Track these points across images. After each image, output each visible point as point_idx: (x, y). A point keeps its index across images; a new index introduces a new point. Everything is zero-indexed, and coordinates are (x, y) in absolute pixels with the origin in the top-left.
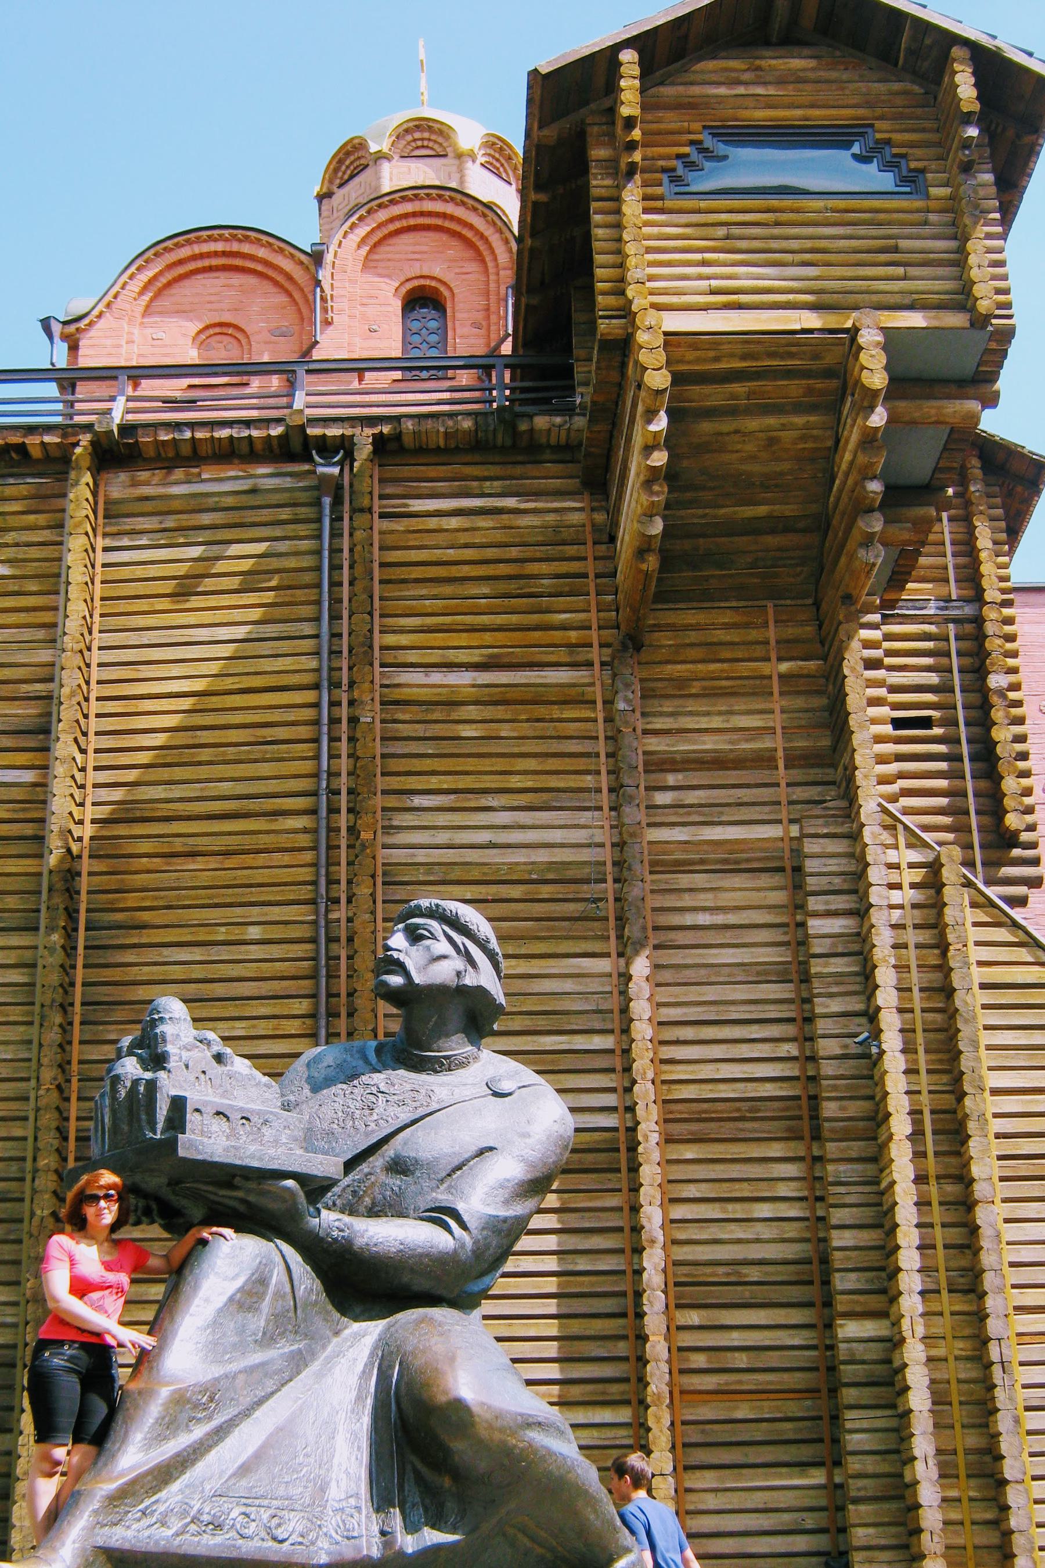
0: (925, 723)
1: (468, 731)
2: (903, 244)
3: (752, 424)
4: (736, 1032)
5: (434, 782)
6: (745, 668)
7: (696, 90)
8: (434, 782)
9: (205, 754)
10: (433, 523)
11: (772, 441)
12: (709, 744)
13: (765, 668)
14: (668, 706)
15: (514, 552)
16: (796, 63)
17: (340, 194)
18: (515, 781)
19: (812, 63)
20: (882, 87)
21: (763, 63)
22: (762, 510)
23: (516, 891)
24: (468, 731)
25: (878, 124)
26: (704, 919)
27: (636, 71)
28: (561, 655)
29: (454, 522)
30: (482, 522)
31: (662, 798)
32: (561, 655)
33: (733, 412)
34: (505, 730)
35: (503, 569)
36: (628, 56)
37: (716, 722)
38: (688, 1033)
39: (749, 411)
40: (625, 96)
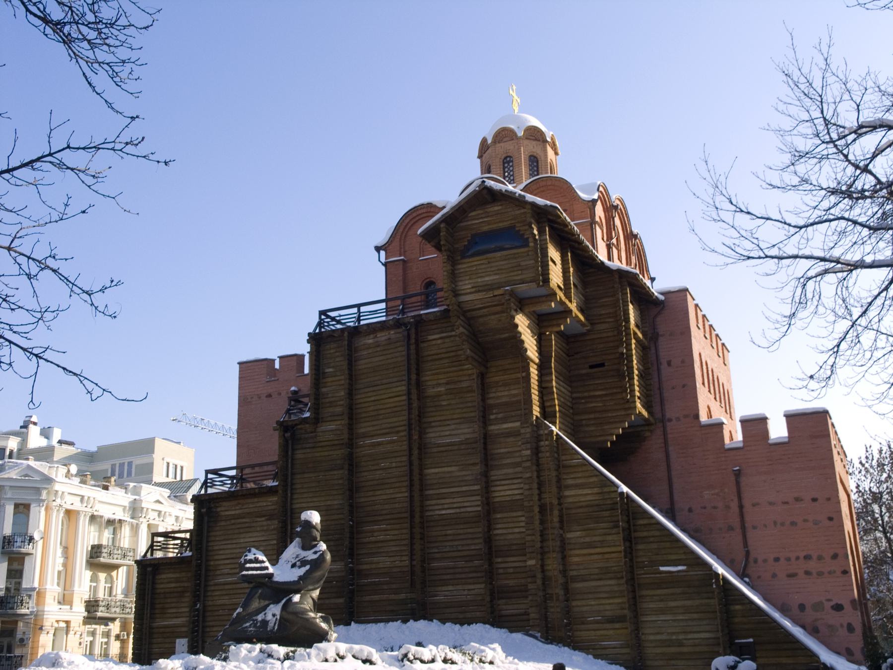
0: (602, 365)
1: (444, 403)
2: (523, 263)
3: (493, 317)
4: (510, 482)
5: (435, 419)
6: (513, 376)
7: (470, 223)
8: (435, 419)
9: (381, 417)
10: (434, 342)
11: (500, 320)
12: (504, 400)
13: (519, 375)
14: (494, 390)
15: (454, 349)
16: (496, 208)
17: (485, 155)
18: (455, 416)
19: (500, 208)
20: (518, 212)
21: (488, 210)
22: (507, 335)
23: (456, 448)
24: (444, 403)
25: (518, 225)
26: (502, 451)
27: (444, 229)
28: (467, 378)
29: (439, 342)
30: (447, 340)
31: (492, 417)
32: (467, 378)
33: (486, 315)
34: (453, 402)
35: (452, 354)
36: (442, 225)
37: (506, 393)
38: (498, 483)
39: (490, 315)
40: (442, 238)
